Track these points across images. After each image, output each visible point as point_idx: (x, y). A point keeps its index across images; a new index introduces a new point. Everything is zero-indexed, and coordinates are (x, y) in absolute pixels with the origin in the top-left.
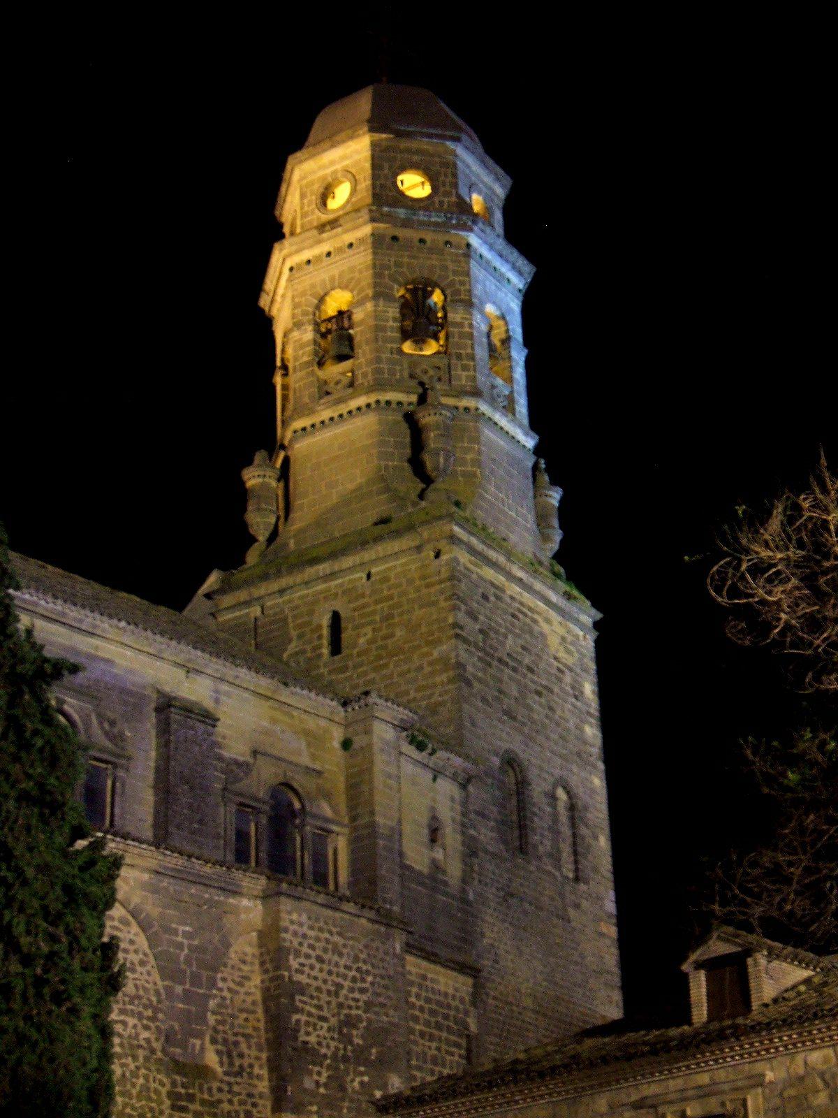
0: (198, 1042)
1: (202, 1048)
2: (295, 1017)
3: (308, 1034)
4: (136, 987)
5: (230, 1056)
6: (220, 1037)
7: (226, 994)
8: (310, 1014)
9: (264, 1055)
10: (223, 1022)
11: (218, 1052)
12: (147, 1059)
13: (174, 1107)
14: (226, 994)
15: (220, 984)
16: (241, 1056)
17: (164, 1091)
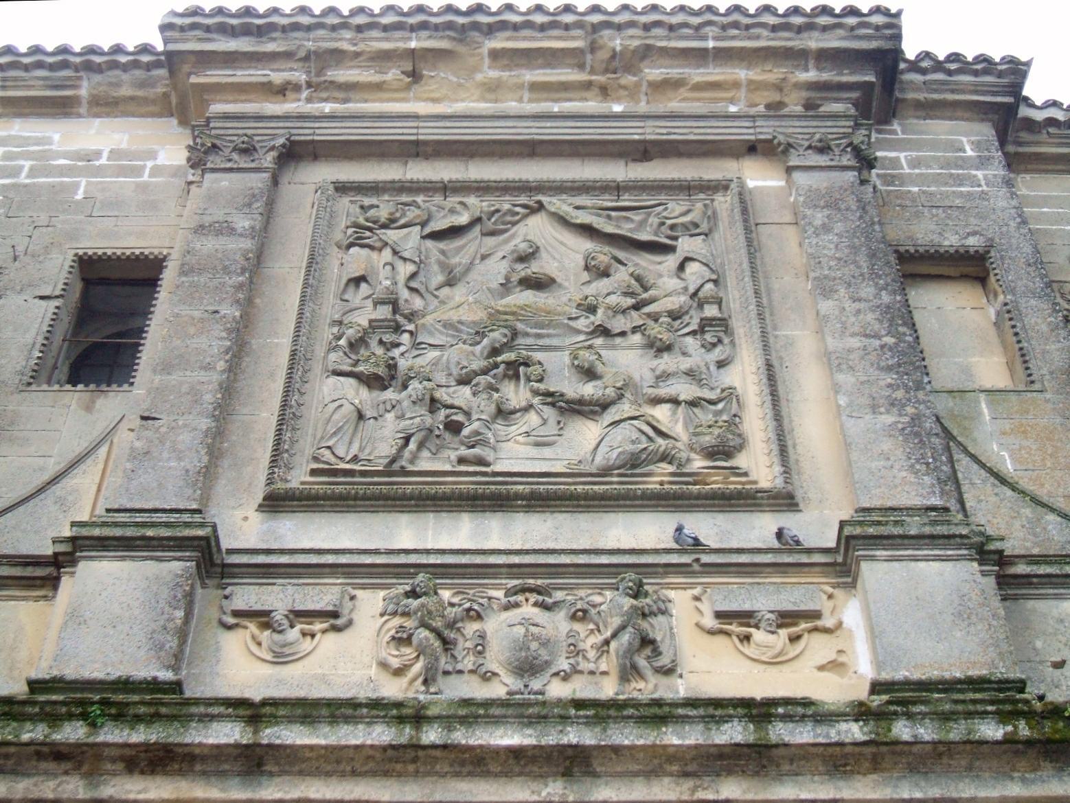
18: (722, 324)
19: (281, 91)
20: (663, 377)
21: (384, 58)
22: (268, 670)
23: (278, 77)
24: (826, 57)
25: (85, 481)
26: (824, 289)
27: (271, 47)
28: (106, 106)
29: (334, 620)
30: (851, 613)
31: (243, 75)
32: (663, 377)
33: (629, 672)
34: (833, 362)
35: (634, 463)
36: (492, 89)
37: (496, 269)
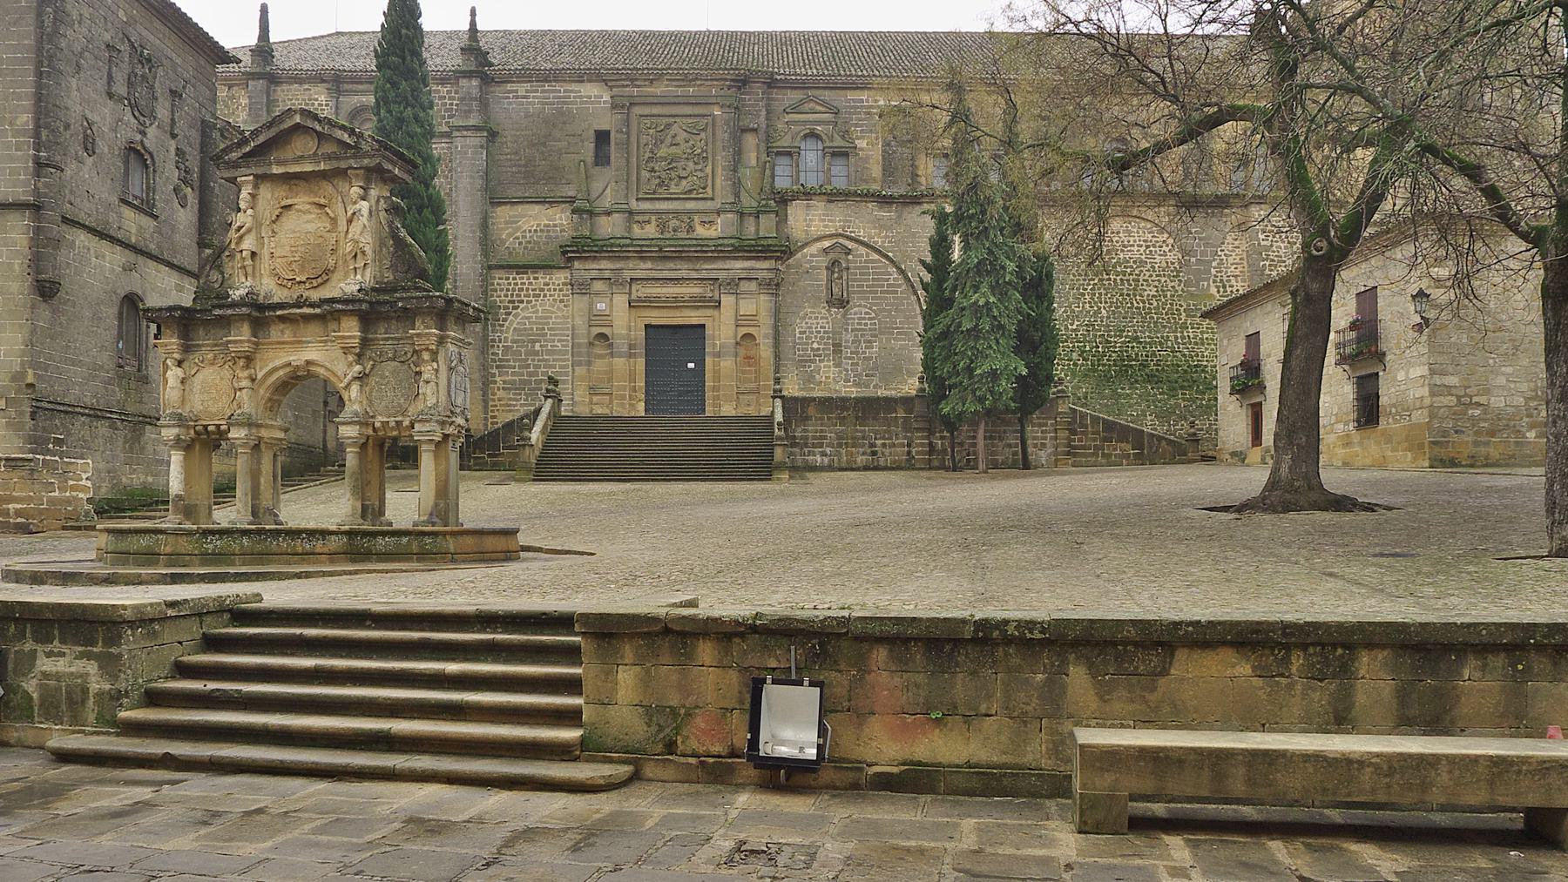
0: (1206, 283)
1: (1209, 285)
2: (1262, 263)
3: (1271, 270)
4: (1167, 263)
5: (1224, 287)
6: (1218, 280)
7: (1223, 257)
8: (1273, 260)
9: (1246, 284)
10: (1221, 272)
11: (1217, 287)
12: (1172, 296)
13: (1187, 316)
14: (1223, 257)
15: (1219, 253)
16: (1232, 286)
17: (1182, 309)
18: (707, 157)
19: (627, 86)
20: (696, 170)
21: (645, 80)
22: (640, 231)
23: (626, 83)
24: (732, 80)
25: (608, 191)
26: (724, 150)
27: (623, 77)
28: (589, 81)
29: (649, 222)
30: (719, 221)
31: (618, 83)
32: (696, 170)
33: (688, 232)
34: (723, 169)
35: (690, 191)
36: (667, 86)
37: (669, 140)
